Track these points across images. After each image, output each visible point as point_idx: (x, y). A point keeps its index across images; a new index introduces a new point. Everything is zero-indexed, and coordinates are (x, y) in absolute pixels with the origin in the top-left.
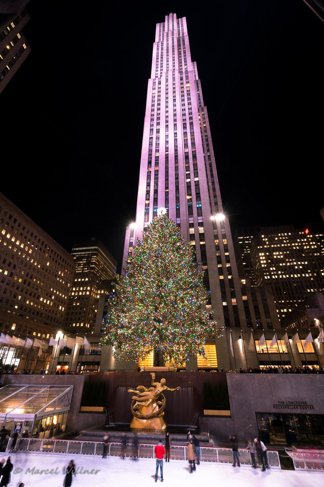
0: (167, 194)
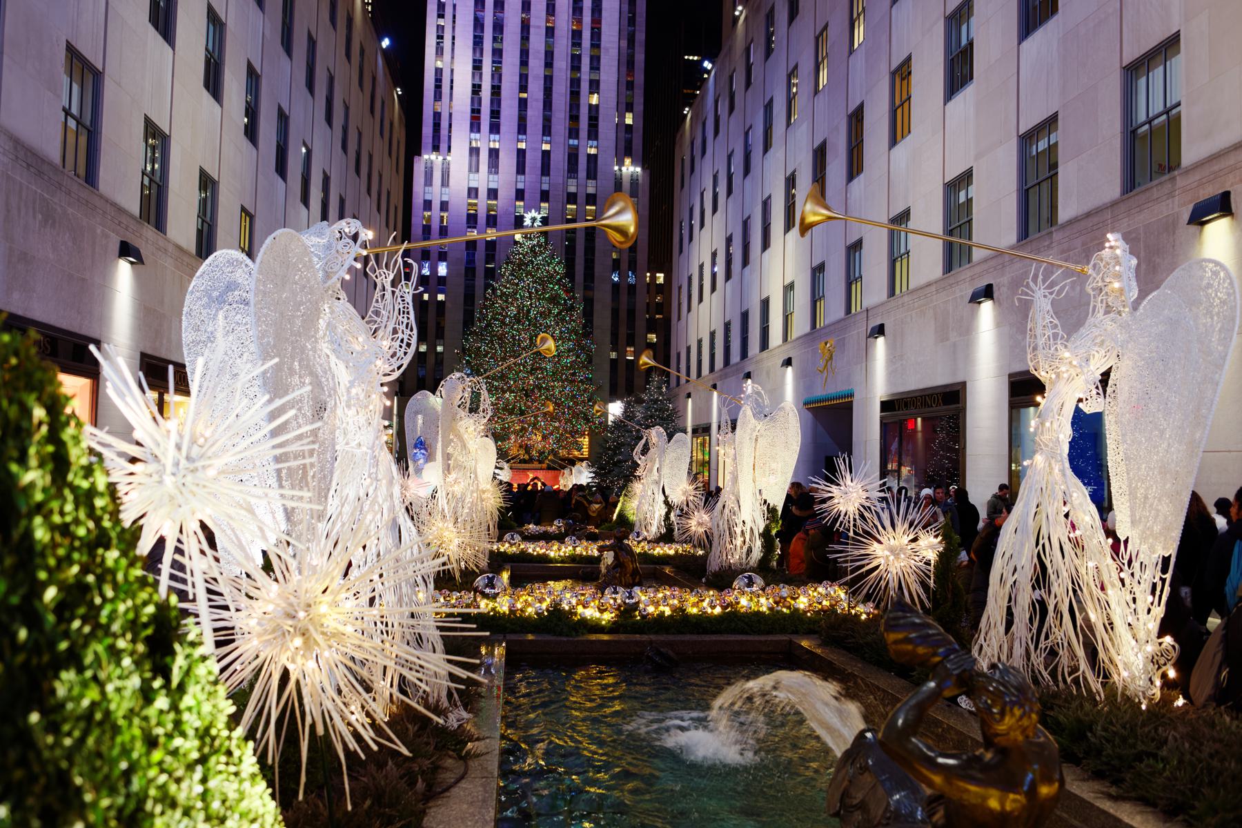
0: (523, 104)
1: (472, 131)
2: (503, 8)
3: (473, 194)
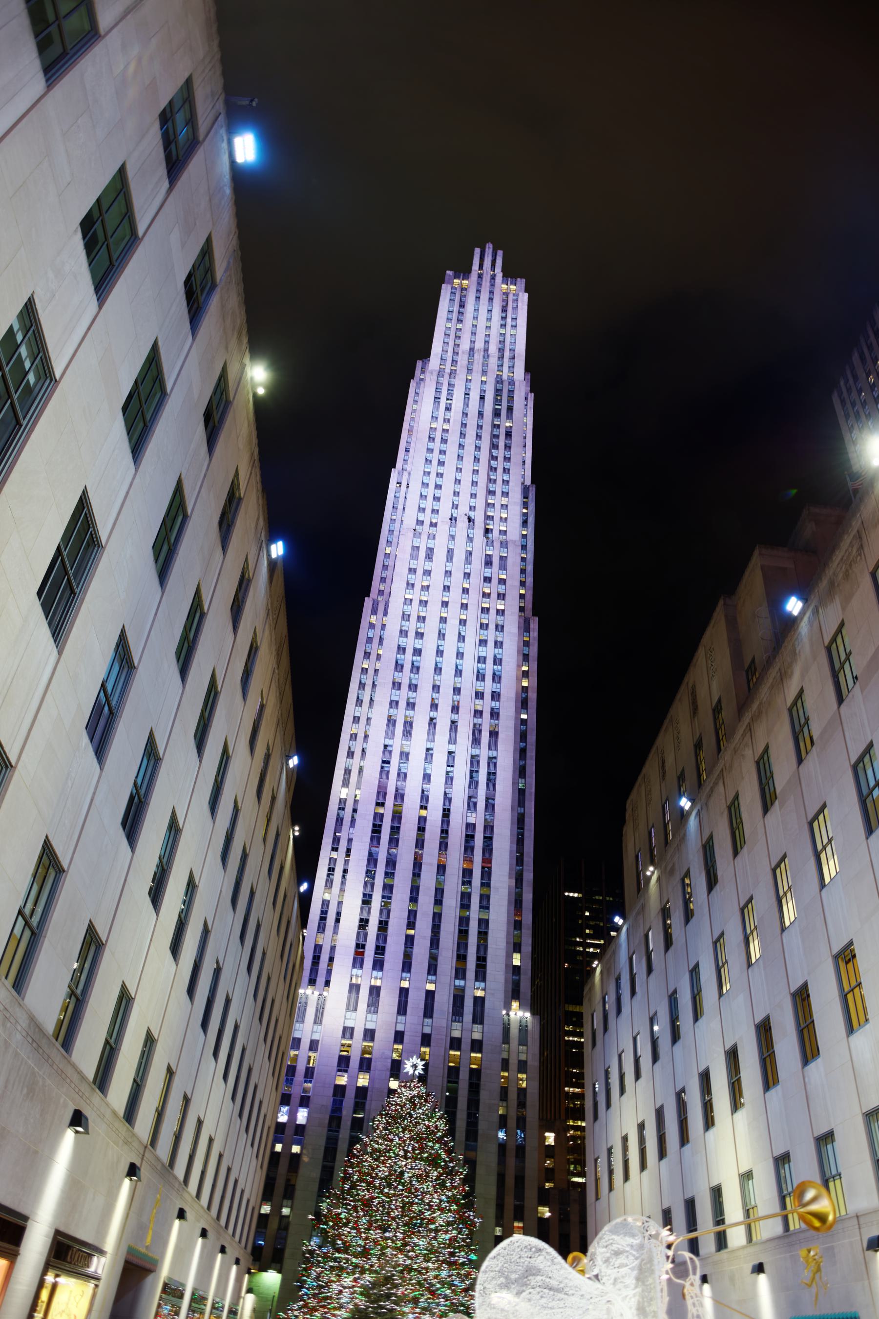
0: (409, 941)
1: (354, 966)
2: (397, 845)
3: (348, 1035)
